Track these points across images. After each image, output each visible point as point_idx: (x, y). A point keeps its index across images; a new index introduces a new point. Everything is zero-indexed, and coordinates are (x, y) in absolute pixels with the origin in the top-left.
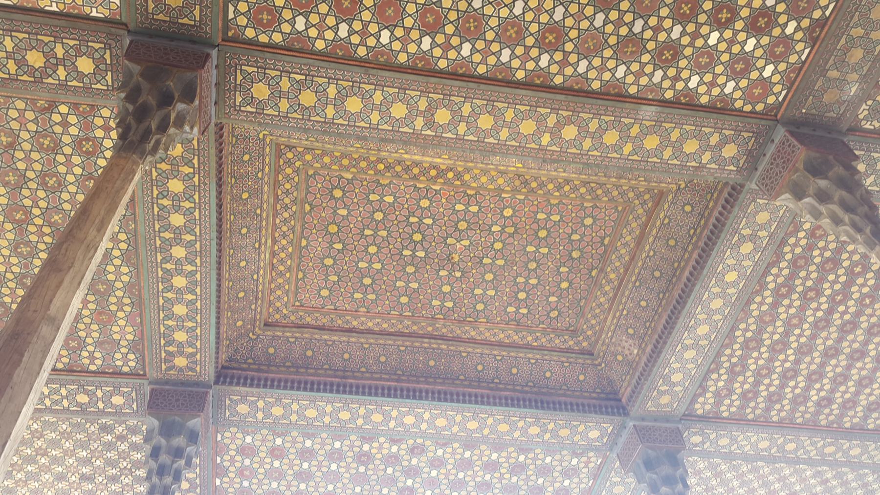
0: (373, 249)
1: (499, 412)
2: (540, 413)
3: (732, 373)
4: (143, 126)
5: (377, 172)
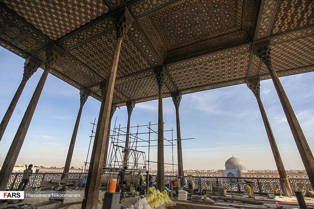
0: (179, 29)
1: (219, 52)
2: (229, 49)
3: (283, 19)
4: (119, 32)
5: (171, 12)
